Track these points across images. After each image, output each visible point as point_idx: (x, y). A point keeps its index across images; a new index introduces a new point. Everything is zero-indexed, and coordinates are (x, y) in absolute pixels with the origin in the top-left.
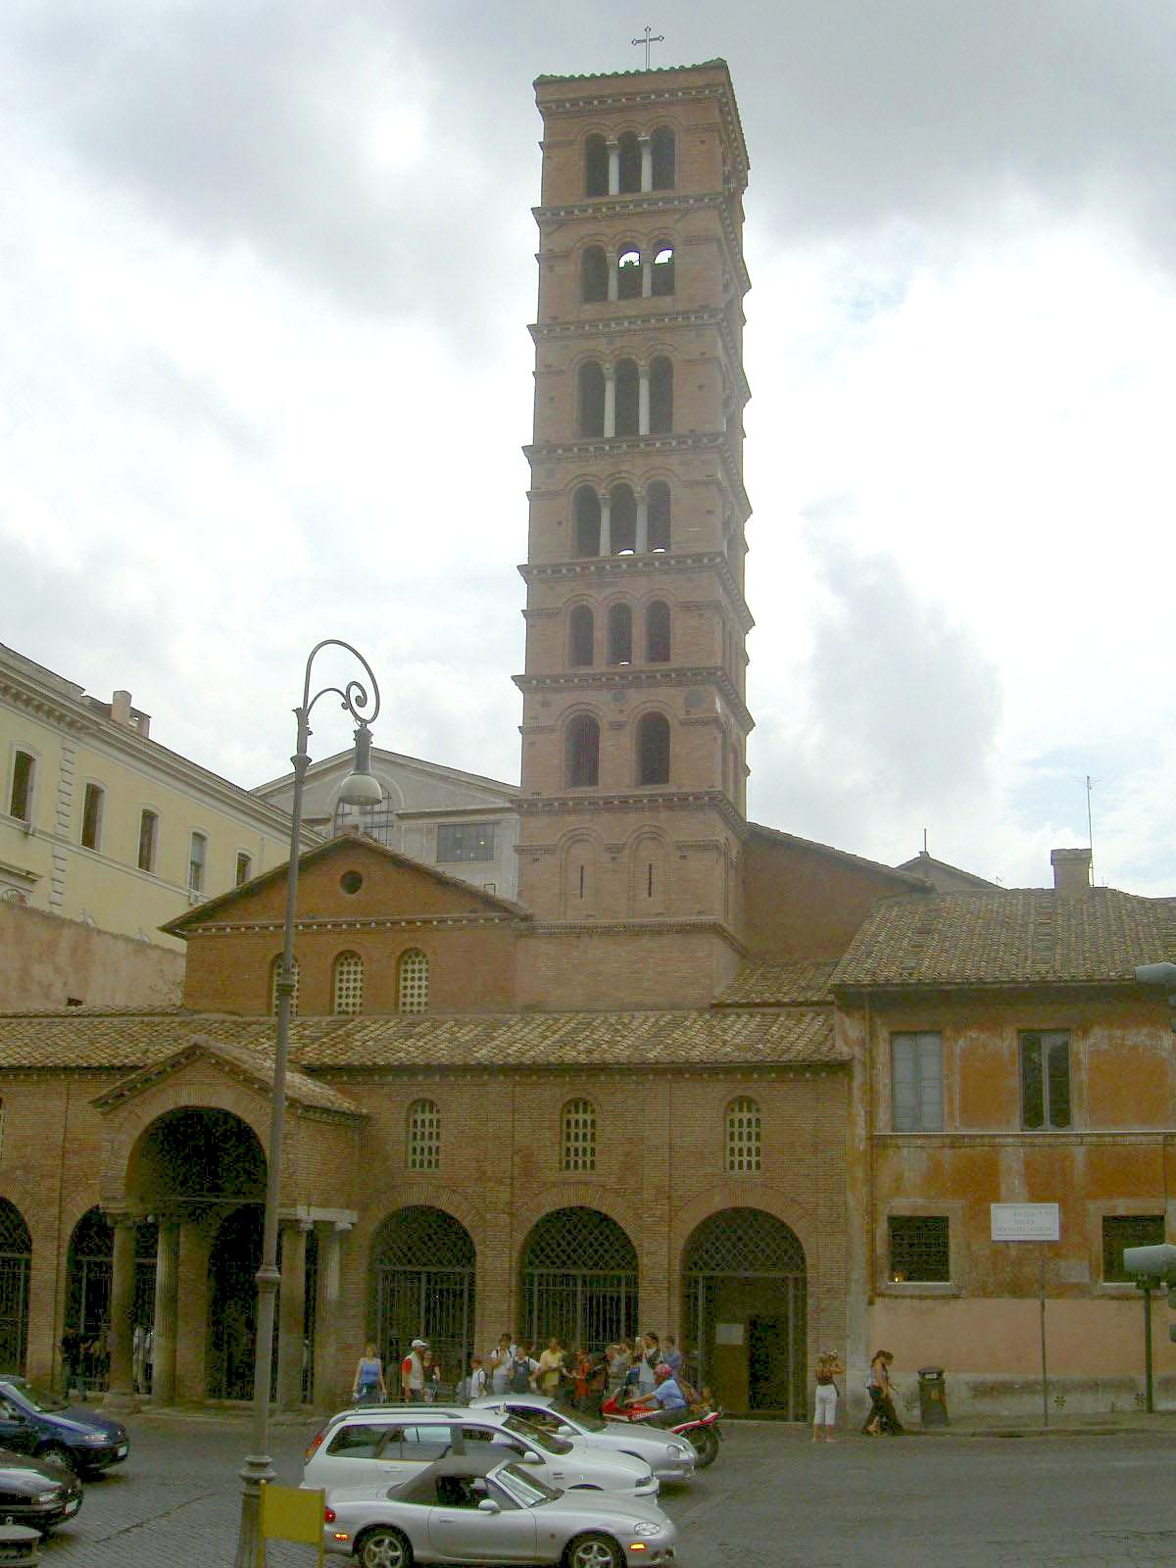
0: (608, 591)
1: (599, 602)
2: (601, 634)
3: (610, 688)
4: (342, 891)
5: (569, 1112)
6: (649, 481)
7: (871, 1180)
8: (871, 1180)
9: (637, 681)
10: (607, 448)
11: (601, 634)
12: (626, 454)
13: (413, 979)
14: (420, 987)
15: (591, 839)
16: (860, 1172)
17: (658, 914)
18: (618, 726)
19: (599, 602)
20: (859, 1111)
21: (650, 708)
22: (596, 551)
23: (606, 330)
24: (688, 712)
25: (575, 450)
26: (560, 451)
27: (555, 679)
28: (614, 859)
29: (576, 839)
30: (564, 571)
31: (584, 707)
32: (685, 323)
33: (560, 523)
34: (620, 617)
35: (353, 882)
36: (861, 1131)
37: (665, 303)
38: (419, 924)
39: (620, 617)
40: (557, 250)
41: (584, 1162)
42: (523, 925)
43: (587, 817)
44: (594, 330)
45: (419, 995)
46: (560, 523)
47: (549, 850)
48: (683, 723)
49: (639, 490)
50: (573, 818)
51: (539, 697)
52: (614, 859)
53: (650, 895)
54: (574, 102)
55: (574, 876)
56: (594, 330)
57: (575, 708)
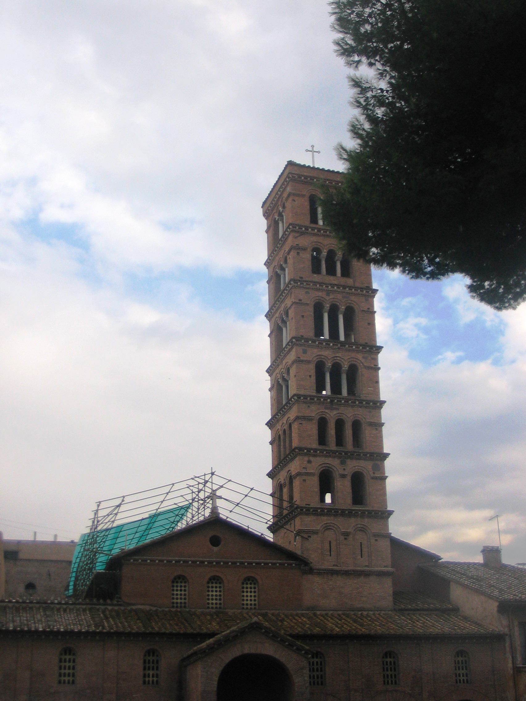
0: (335, 412)
1: (332, 416)
2: (332, 432)
3: (340, 458)
4: (209, 544)
5: (387, 657)
6: (334, 361)
7: (516, 685)
8: (516, 685)
9: (351, 456)
10: (331, 344)
11: (332, 432)
12: (339, 348)
13: (247, 592)
14: (251, 596)
15: (334, 529)
16: (511, 684)
17: (366, 566)
18: (343, 476)
19: (332, 416)
20: (509, 656)
21: (357, 469)
22: (340, 393)
23: (326, 288)
24: (374, 473)
25: (317, 343)
26: (310, 342)
27: (315, 450)
28: (345, 539)
29: (327, 528)
30: (316, 399)
31: (328, 465)
32: (361, 293)
33: (310, 376)
34: (340, 424)
35: (215, 541)
36: (510, 665)
37: (349, 281)
38: (238, 564)
39: (340, 424)
40: (300, 245)
41: (392, 681)
42: (307, 568)
43: (332, 518)
44: (321, 288)
45: (251, 600)
46: (310, 376)
47: (315, 532)
48: (373, 478)
49: (345, 367)
50: (325, 518)
51: (306, 458)
52: (345, 539)
53: (362, 557)
54: (306, 177)
55: (327, 546)
56: (321, 288)
57: (323, 465)
